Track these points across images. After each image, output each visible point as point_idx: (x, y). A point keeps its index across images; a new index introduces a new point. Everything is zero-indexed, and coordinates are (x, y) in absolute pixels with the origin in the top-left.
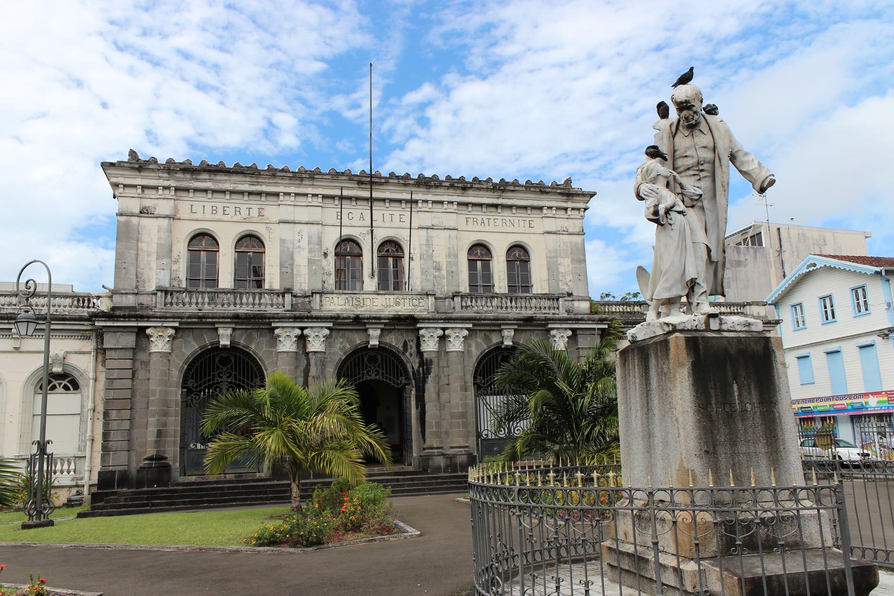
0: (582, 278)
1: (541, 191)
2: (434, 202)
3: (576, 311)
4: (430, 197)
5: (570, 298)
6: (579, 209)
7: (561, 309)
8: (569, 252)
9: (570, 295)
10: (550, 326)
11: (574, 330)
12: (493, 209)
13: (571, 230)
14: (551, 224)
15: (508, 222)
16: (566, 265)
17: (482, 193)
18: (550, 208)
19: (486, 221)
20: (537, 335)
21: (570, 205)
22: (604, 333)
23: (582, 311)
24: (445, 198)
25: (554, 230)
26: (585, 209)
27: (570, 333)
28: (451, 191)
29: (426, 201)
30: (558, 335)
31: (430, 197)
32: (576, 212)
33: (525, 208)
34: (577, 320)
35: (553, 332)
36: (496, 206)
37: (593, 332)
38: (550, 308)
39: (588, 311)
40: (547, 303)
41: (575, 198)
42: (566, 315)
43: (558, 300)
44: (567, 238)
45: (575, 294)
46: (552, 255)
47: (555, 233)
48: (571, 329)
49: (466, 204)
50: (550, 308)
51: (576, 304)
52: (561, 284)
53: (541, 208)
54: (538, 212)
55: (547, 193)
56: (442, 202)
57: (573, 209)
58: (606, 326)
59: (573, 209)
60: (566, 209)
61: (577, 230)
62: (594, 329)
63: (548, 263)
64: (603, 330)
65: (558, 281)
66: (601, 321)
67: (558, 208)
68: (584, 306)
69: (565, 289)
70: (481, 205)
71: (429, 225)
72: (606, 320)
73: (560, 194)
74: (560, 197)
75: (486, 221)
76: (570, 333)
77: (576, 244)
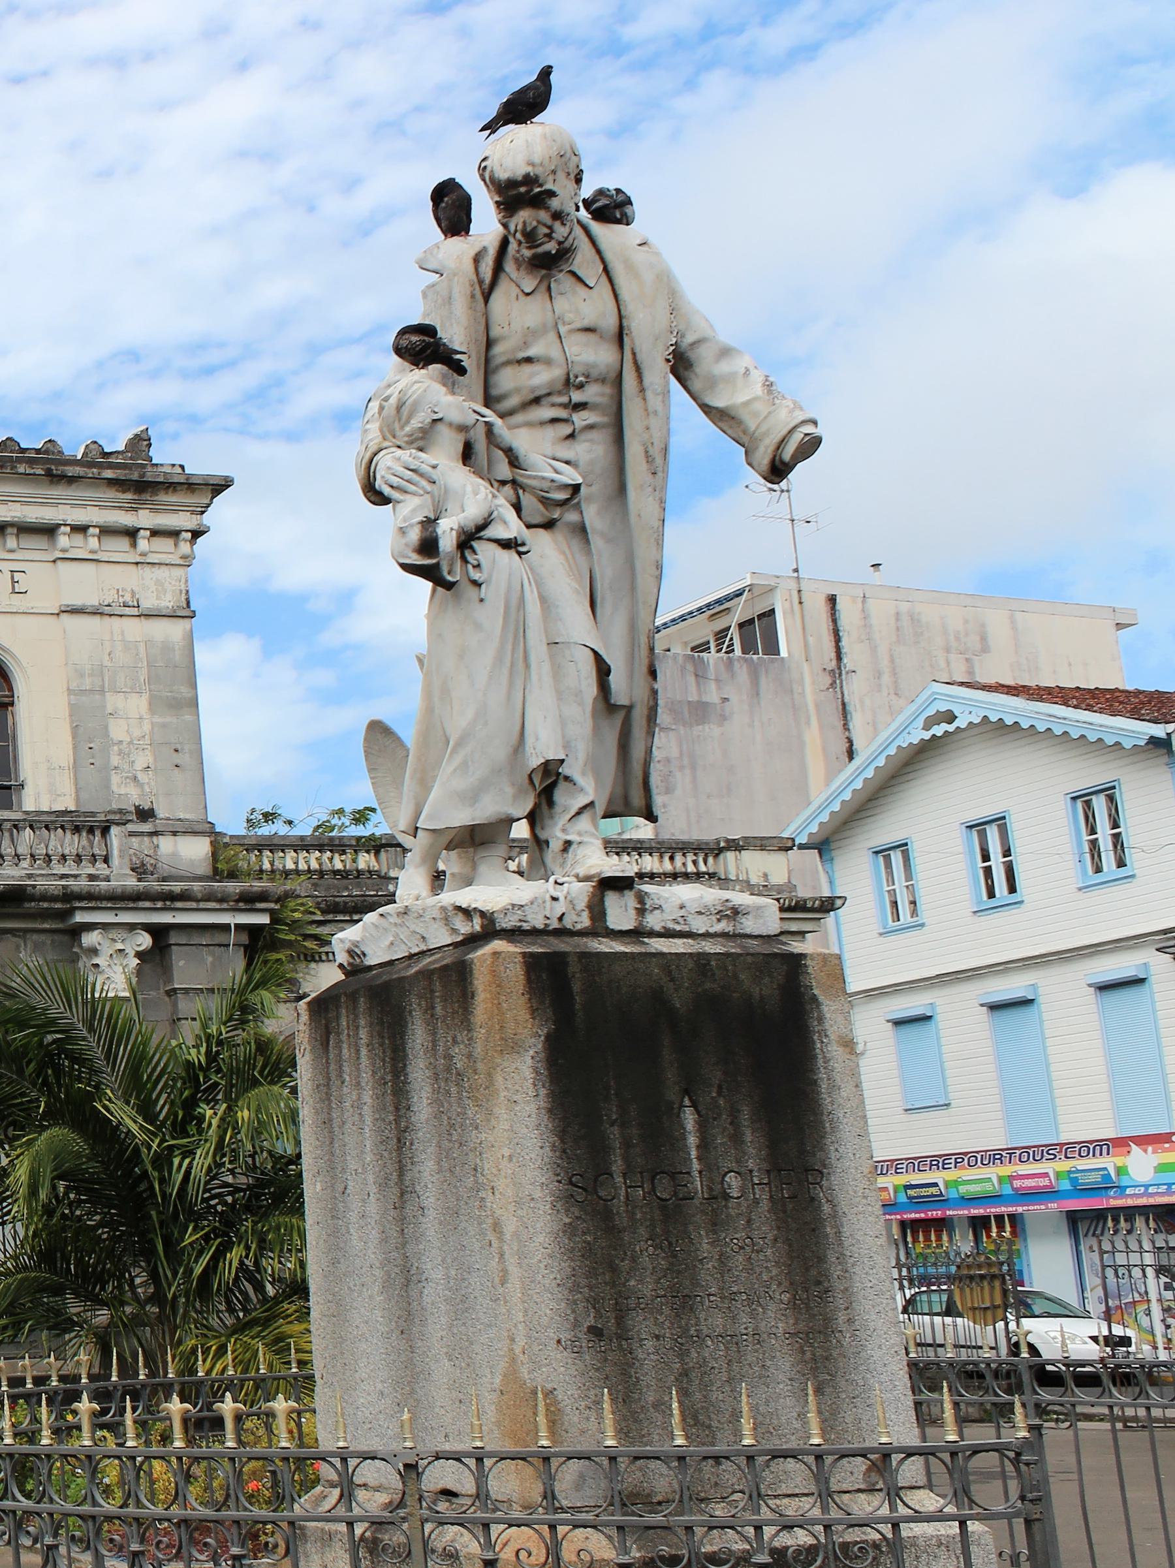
0: (184, 759)
1: (49, 474)
3: (164, 870)
5: (146, 827)
6: (174, 534)
7: (115, 860)
8: (143, 675)
9: (145, 814)
10: (80, 918)
11: (158, 932)
13: (148, 603)
14: (84, 584)
16: (131, 716)
18: (80, 529)
20: (37, 948)
21: (144, 519)
22: (256, 942)
23: (184, 868)
25: (92, 601)
26: (196, 534)
27: (145, 941)
30: (107, 949)
32: (166, 544)
34: (170, 899)
35: (90, 939)
37: (220, 938)
38: (79, 859)
39: (205, 869)
40: (71, 843)
41: (163, 497)
42: (131, 882)
43: (105, 831)
44: (134, 629)
45: (161, 813)
46: (87, 684)
47: (96, 612)
48: (150, 928)
50: (79, 859)
51: (166, 844)
52: (115, 779)
53: (49, 531)
54: (40, 542)
55: (71, 480)
57: (155, 533)
58: (265, 919)
59: (155, 533)
60: (131, 534)
61: (167, 602)
62: (225, 928)
63: (74, 710)
64: (253, 931)
65: (106, 770)
66: (249, 901)
67: (107, 531)
68: (193, 852)
69: (129, 795)
72: (263, 897)
73: (112, 482)
74: (112, 494)
76: (145, 941)
77: (167, 647)
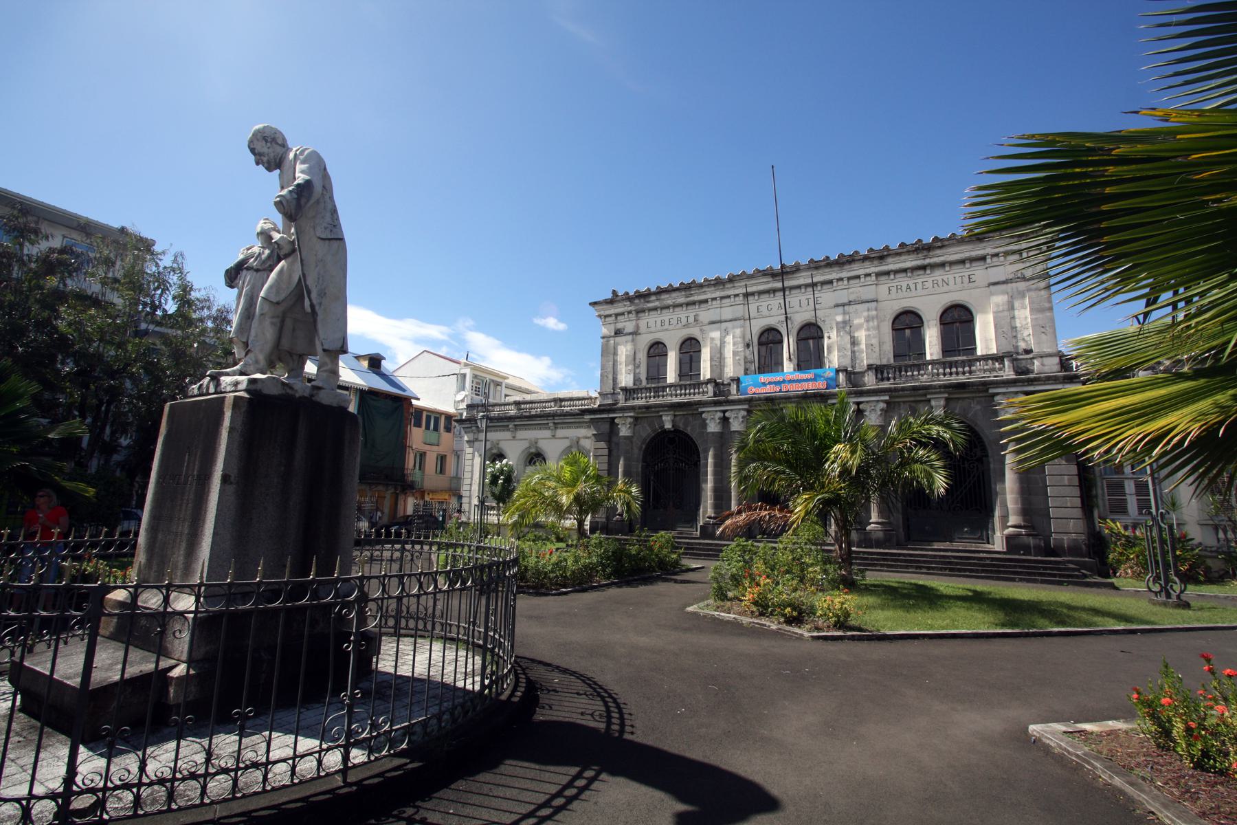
2: (849, 279)
4: (844, 274)
12: (921, 272)
15: (940, 283)
17: (903, 257)
18: (997, 255)
19: (913, 287)
20: (978, 403)
24: (861, 272)
25: (1004, 279)
28: (867, 263)
29: (841, 279)
31: (844, 274)
33: (962, 262)
36: (923, 268)
49: (888, 273)
54: (982, 263)
56: (858, 277)
70: (905, 271)
71: (846, 301)
75: (913, 287)
